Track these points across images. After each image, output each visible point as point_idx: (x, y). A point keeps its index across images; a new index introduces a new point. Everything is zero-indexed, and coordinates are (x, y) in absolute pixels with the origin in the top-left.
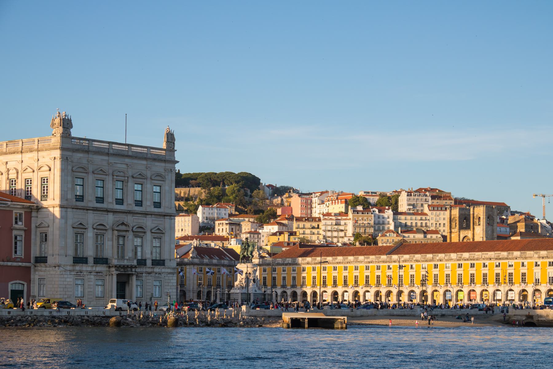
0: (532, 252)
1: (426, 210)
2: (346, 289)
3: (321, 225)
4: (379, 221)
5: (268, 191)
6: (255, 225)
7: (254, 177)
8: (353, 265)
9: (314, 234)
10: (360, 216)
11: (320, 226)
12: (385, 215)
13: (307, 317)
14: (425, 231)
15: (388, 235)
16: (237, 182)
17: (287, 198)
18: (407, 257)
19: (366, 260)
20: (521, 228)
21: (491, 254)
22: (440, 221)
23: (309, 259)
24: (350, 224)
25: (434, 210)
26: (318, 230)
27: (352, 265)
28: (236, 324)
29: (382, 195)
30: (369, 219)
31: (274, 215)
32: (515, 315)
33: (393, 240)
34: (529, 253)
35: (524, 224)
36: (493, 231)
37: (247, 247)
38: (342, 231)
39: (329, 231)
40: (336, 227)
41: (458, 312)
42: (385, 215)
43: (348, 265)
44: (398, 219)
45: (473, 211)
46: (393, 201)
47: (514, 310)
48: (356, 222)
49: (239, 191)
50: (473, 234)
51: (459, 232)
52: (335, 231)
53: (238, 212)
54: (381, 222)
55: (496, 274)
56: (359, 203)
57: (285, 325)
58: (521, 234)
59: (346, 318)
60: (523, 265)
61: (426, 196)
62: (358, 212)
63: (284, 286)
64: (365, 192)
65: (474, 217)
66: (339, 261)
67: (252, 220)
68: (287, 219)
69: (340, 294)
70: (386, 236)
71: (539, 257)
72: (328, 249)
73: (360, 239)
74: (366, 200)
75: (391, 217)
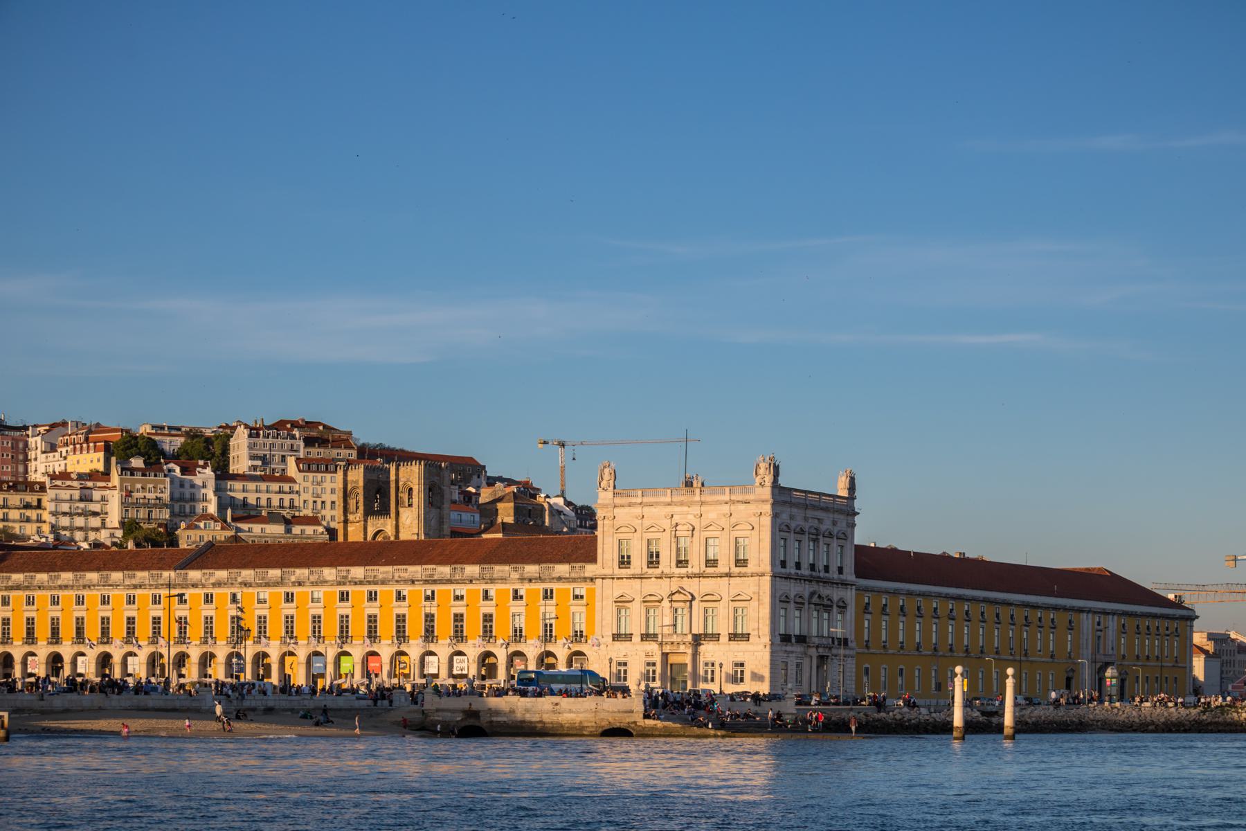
0: (506, 568)
1: (292, 470)
2: (82, 648)
3: (46, 500)
4: (182, 494)
8: (96, 594)
9: (28, 520)
10: (138, 481)
11: (45, 503)
12: (198, 480)
14: (289, 517)
15: (202, 525)
18: (222, 574)
19: (127, 582)
20: (506, 513)
21: (415, 570)
22: (321, 494)
24: (115, 499)
25: (309, 470)
26: (39, 511)
27: (95, 592)
29: (193, 435)
30: (158, 489)
32: (438, 710)
34: (500, 570)
35: (512, 504)
36: (441, 521)
38: (95, 514)
39: (65, 514)
40: (82, 505)
41: (306, 702)
42: (198, 480)
43: (85, 593)
44: (226, 490)
45: (397, 475)
46: (217, 449)
47: (436, 699)
48: (129, 494)
50: (397, 527)
51: (366, 521)
52: (79, 515)
54: (188, 496)
58: (505, 527)
60: (486, 596)
61: (293, 437)
62: (133, 471)
64: (153, 427)
66: (65, 583)
69: (67, 659)
70: (197, 527)
71: (522, 579)
72: (58, 555)
73: (136, 533)
74: (152, 444)
75: (211, 484)
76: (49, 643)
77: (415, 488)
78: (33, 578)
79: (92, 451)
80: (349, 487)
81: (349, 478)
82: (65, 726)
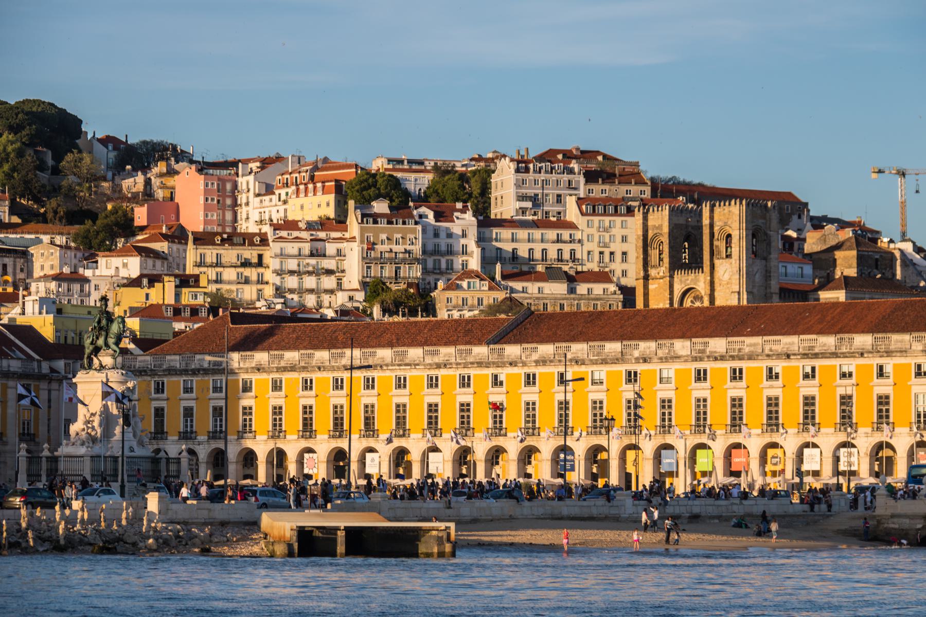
0: (906, 337)
1: (572, 212)
2: (371, 443)
4: (437, 246)
5: (107, 155)
6: (70, 254)
7: (63, 112)
8: (390, 375)
9: (247, 281)
10: (383, 230)
11: (267, 260)
13: (342, 525)
14: (572, 273)
15: (465, 284)
16: (14, 129)
17: (161, 175)
18: (546, 349)
19: (429, 360)
20: (847, 264)
23: (261, 357)
25: (594, 213)
26: (260, 270)
27: (388, 373)
28: (134, 544)
29: (443, 171)
30: (407, 239)
31: (127, 228)
33: (480, 301)
34: (898, 339)
35: (854, 253)
36: (767, 276)
37: (104, 322)
38: (329, 272)
39: (292, 273)
40: (313, 261)
41: (735, 508)
44: (491, 240)
45: (712, 218)
47: (891, 502)
48: (371, 246)
49: (20, 154)
50: (712, 283)
51: (671, 277)
52: (310, 273)
53: (19, 216)
54: (443, 248)
55: (806, 398)
56: (371, 191)
57: (280, 549)
58: (847, 282)
59: (452, 525)
60: (881, 373)
61: (571, 171)
62: (375, 218)
63: (187, 435)
64: (389, 161)
65: (712, 235)
67: (60, 240)
68: (165, 237)
70: (458, 287)
73: (384, 296)
74: (395, 183)
75: (473, 232)
76: (330, 437)
77: (735, 234)
78: (310, 356)
79: (319, 193)
80: (650, 234)
81: (650, 223)
82: (505, 539)
